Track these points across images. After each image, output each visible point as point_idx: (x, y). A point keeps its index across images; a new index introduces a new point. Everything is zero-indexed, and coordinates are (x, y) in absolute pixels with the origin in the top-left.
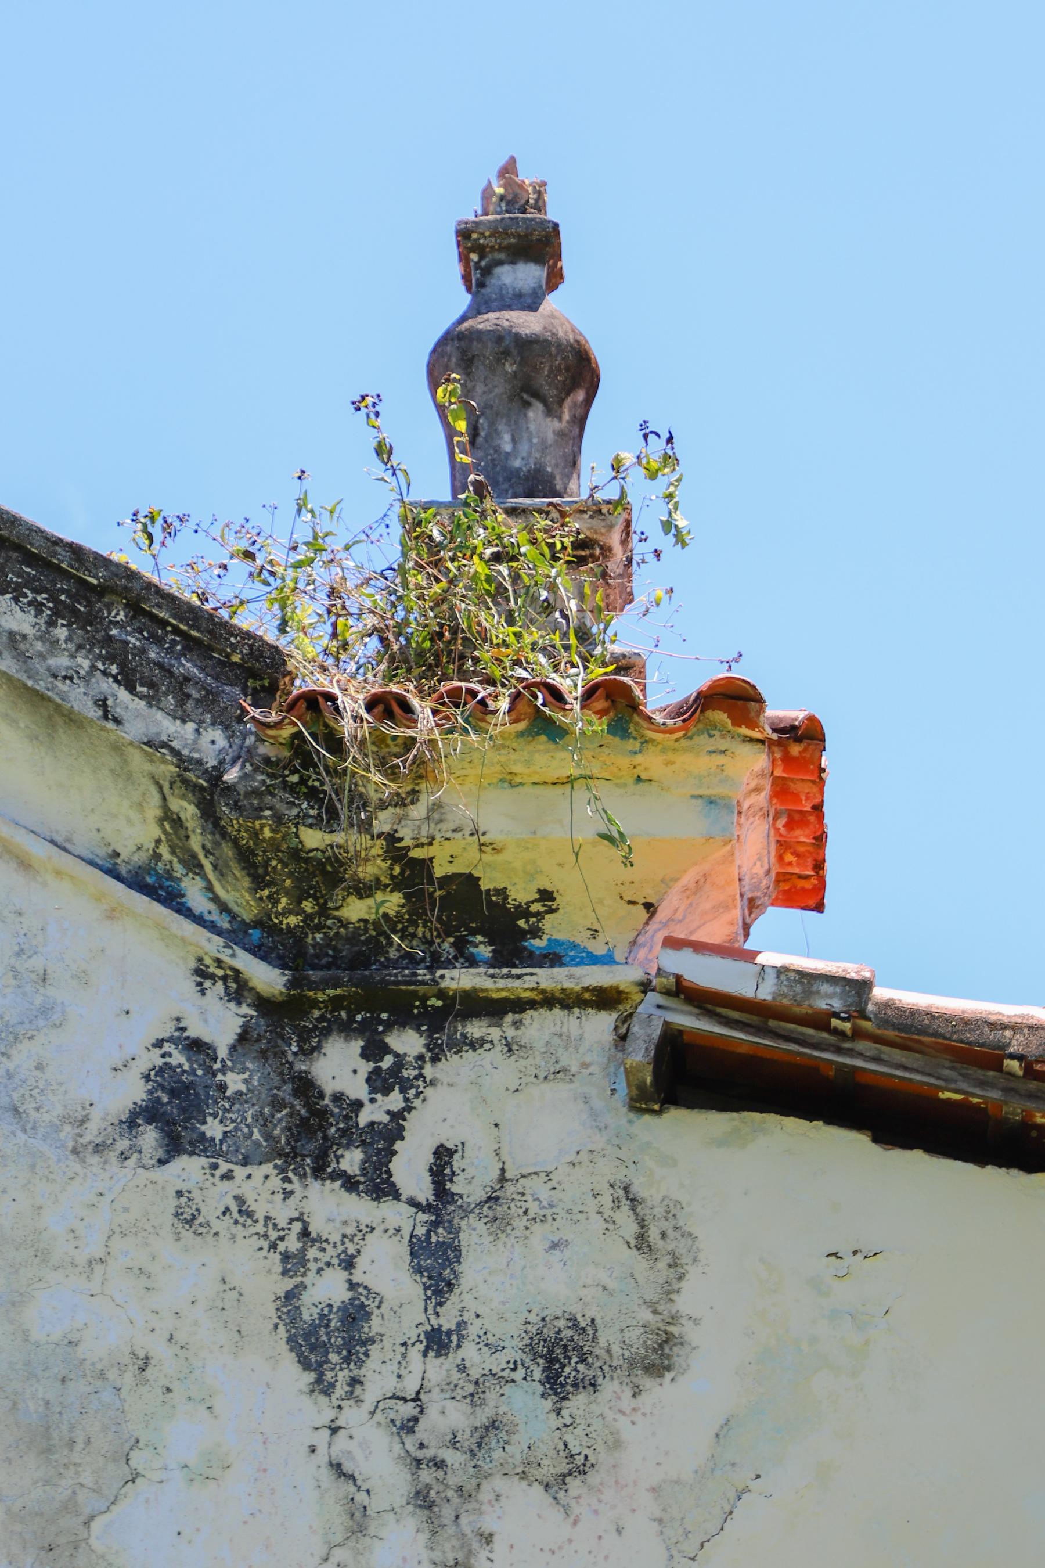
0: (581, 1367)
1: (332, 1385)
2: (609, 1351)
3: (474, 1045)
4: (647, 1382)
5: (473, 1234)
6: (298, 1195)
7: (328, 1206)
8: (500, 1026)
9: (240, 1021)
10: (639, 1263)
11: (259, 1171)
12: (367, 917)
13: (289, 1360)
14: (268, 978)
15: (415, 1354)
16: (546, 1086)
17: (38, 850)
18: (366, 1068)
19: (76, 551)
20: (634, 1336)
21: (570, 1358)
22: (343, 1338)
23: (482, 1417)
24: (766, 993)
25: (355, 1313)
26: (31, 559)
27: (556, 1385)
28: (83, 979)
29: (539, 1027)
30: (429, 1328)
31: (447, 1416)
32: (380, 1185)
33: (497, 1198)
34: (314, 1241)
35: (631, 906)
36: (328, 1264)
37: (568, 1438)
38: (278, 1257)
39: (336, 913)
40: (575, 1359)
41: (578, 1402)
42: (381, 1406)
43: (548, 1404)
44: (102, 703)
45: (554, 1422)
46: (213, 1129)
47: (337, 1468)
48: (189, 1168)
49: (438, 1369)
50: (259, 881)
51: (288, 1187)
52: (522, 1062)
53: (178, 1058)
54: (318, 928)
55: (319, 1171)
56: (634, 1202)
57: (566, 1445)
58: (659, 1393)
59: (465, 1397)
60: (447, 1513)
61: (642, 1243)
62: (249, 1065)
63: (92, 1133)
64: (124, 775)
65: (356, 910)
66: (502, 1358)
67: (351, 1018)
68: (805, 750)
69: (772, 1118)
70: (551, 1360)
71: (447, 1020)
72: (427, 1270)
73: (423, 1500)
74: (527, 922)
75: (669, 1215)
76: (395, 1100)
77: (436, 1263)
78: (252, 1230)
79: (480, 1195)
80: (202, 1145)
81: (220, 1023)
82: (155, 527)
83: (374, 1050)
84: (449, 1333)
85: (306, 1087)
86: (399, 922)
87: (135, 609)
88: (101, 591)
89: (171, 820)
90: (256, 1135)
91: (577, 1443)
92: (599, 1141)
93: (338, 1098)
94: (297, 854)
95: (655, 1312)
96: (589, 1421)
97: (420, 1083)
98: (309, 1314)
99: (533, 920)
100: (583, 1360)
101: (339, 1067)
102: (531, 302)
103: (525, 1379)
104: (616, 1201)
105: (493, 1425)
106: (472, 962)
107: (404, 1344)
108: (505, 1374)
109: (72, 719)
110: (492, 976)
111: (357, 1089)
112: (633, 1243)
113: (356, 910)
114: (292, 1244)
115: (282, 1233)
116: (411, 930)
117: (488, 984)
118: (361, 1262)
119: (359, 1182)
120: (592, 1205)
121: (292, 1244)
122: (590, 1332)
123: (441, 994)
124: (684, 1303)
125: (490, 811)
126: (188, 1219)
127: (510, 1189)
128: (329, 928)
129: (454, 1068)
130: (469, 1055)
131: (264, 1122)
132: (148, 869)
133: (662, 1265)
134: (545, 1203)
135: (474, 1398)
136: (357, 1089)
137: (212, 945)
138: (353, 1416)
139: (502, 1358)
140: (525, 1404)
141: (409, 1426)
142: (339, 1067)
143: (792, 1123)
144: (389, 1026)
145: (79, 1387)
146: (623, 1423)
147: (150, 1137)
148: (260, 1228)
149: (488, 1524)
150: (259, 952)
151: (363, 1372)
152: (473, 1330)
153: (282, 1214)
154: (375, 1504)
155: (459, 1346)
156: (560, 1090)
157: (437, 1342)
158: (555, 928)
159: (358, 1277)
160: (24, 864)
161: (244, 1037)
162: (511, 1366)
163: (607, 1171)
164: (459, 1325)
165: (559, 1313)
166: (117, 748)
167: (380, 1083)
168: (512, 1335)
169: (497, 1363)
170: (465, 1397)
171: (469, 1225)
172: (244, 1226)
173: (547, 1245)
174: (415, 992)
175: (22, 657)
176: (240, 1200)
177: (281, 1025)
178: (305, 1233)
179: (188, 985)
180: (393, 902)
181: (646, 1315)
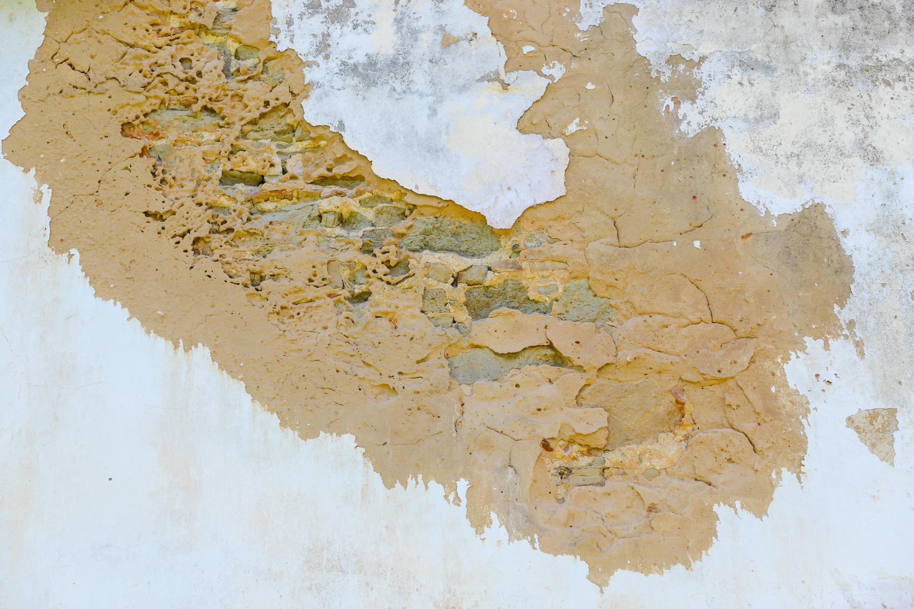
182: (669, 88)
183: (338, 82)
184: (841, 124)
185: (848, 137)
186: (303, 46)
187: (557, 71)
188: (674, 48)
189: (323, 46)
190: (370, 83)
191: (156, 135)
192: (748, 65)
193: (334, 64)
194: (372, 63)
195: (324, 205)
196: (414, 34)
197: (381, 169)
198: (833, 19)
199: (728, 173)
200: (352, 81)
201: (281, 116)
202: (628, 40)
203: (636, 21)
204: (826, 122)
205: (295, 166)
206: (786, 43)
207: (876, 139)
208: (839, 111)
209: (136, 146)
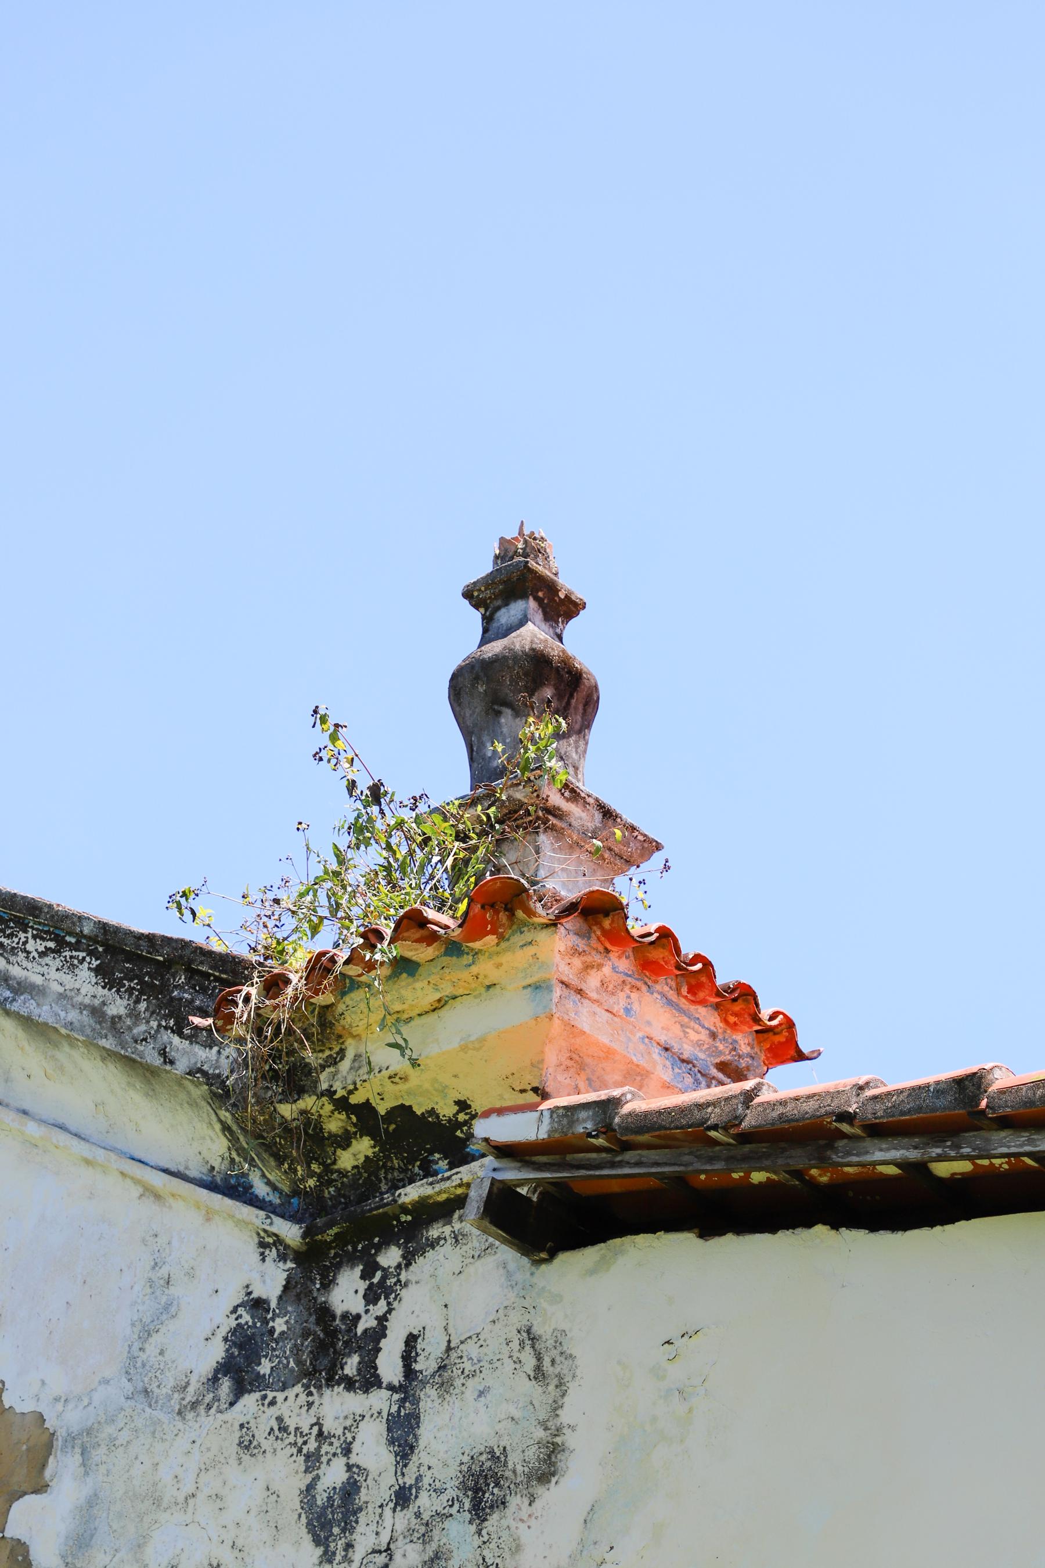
0: (496, 1491)
1: (334, 1553)
2: (514, 1472)
3: (433, 1244)
4: (540, 1490)
5: (429, 1399)
6: (316, 1404)
7: (336, 1405)
8: (450, 1223)
9: (285, 1275)
11: (291, 1393)
12: (356, 1163)
13: (308, 1538)
15: (388, 1511)
16: (479, 1263)
17: (158, 1180)
19: (150, 938)
20: (531, 1453)
21: (489, 1485)
22: (342, 1513)
25: (350, 1490)
30: (397, 1487)
32: (368, 1380)
33: (445, 1366)
34: (326, 1438)
35: (524, 1094)
36: (334, 1455)
37: (486, 1553)
38: (303, 1458)
39: (336, 1167)
40: (492, 1485)
41: (494, 1519)
42: (365, 1562)
43: (473, 1528)
44: (163, 1053)
45: (477, 1541)
49: (403, 1520)
50: (280, 1160)
51: (310, 1399)
52: (464, 1248)
53: (246, 1318)
54: (330, 1182)
55: (331, 1382)
56: (533, 1339)
57: (484, 1559)
58: (549, 1495)
59: (419, 1539)
61: (539, 1374)
62: (290, 1309)
63: (190, 1396)
65: (347, 1160)
66: (444, 1498)
67: (355, 1248)
68: (613, 921)
69: (628, 1240)
70: (476, 1490)
72: (398, 1440)
74: (462, 1132)
75: (558, 1343)
76: (381, 1307)
78: (287, 1441)
79: (433, 1366)
80: (258, 1383)
81: (271, 1280)
82: (181, 901)
83: (370, 1269)
84: (411, 1486)
85: (324, 1313)
86: (379, 1160)
88: (167, 966)
90: (292, 1364)
91: (491, 1555)
93: (345, 1316)
94: (286, 1128)
95: (546, 1429)
96: (500, 1534)
97: (398, 1287)
98: (321, 1499)
99: (465, 1128)
100: (497, 1485)
101: (347, 1293)
103: (459, 1511)
104: (522, 1344)
105: (437, 1556)
107: (381, 1506)
108: (446, 1511)
110: (431, 1184)
112: (532, 1374)
113: (347, 1160)
114: (312, 1445)
115: (306, 1438)
116: (389, 1164)
117: (429, 1191)
118: (356, 1447)
119: (356, 1381)
120: (506, 1350)
121: (312, 1445)
122: (503, 1459)
123: (404, 1209)
124: (566, 1416)
127: (454, 1355)
128: (336, 1181)
129: (423, 1265)
130: (430, 1254)
133: (551, 1388)
134: (475, 1361)
135: (425, 1539)
139: (444, 1498)
143: (642, 1239)
144: (379, 1248)
146: (523, 1527)
147: (226, 1385)
148: (292, 1439)
151: (354, 1536)
152: (426, 1480)
153: (305, 1421)
155: (416, 1497)
159: (354, 1459)
160: (157, 1197)
161: (286, 1288)
162: (450, 1503)
163: (517, 1319)
164: (417, 1479)
165: (483, 1449)
167: (371, 1297)
169: (439, 1504)
170: (419, 1539)
171: (425, 1394)
172: (282, 1440)
173: (477, 1393)
174: (385, 1214)
176: (280, 1419)
178: (320, 1433)
180: (364, 1147)
181: (540, 1434)
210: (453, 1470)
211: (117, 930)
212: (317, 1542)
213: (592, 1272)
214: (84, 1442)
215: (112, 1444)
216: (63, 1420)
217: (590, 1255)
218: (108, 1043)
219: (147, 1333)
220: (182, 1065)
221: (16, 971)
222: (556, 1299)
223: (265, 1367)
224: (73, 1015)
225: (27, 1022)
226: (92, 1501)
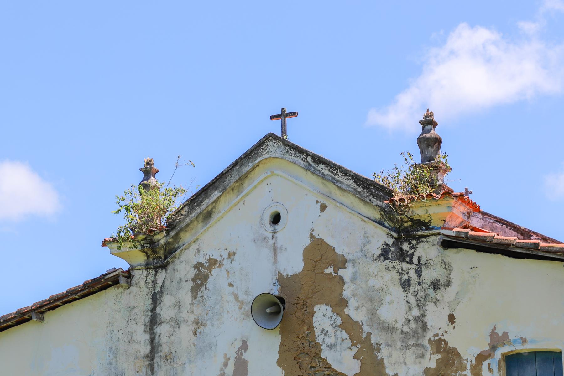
3: (423, 242)
5: (423, 268)
7: (405, 266)
10: (445, 271)
14: (395, 235)
17: (366, 219)
18: (409, 246)
19: (366, 179)
20: (445, 281)
23: (425, 294)
24: (454, 235)
25: (409, 280)
26: (361, 181)
27: (435, 289)
28: (373, 236)
29: (431, 239)
31: (421, 294)
32: (411, 263)
41: (438, 291)
44: (370, 200)
46: (390, 256)
47: (407, 302)
48: (387, 262)
53: (385, 247)
55: (403, 261)
56: (444, 262)
58: (448, 289)
60: (421, 307)
61: (445, 268)
64: (375, 209)
65: (406, 225)
71: (419, 239)
73: (418, 305)
76: (413, 250)
77: (419, 273)
80: (389, 259)
81: (390, 241)
83: (410, 244)
85: (401, 249)
87: (374, 186)
89: (381, 214)
92: (439, 254)
93: (406, 251)
101: (406, 246)
102: (429, 131)
105: (427, 295)
106: (422, 230)
109: (367, 202)
111: (408, 249)
114: (400, 271)
121: (400, 271)
124: (451, 276)
125: (419, 212)
126: (387, 269)
129: (420, 245)
131: (396, 255)
132: (379, 221)
136: (408, 249)
137: (388, 231)
138: (409, 294)
140: (431, 291)
141: (416, 296)
142: (406, 246)
145: (375, 293)
147: (382, 258)
149: (427, 308)
150: (395, 231)
153: (399, 267)
154: (412, 306)
156: (434, 247)
157: (419, 284)
158: (433, 224)
160: (365, 222)
161: (393, 243)
163: (441, 258)
166: (373, 206)
168: (429, 282)
175: (360, 195)
177: (398, 241)
179: (386, 236)
182: (376, 350)
183: (326, 349)
184: (401, 357)
185: (402, 360)
186: (320, 341)
187: (359, 346)
188: (377, 342)
189: (324, 342)
190: (331, 349)
191: (300, 359)
192: (388, 345)
193: (325, 345)
194: (331, 345)
195: (325, 373)
196: (337, 338)
197: (333, 367)
198: (401, 336)
199: (384, 367)
200: (328, 348)
201: (317, 355)
202: (370, 340)
203: (372, 336)
204: (399, 357)
205: (321, 365)
206: (394, 341)
207: (407, 361)
208: (401, 355)
209: (296, 362)
210: (429, 281)
211: (359, 176)
212: (403, 288)
213: (455, 253)
214: (354, 262)
215: (359, 263)
216: (349, 257)
217: (455, 250)
218: (358, 196)
219: (365, 245)
220: (374, 204)
221: (336, 178)
222: (449, 256)
223: (390, 256)
224: (350, 189)
225: (339, 188)
226: (356, 272)
